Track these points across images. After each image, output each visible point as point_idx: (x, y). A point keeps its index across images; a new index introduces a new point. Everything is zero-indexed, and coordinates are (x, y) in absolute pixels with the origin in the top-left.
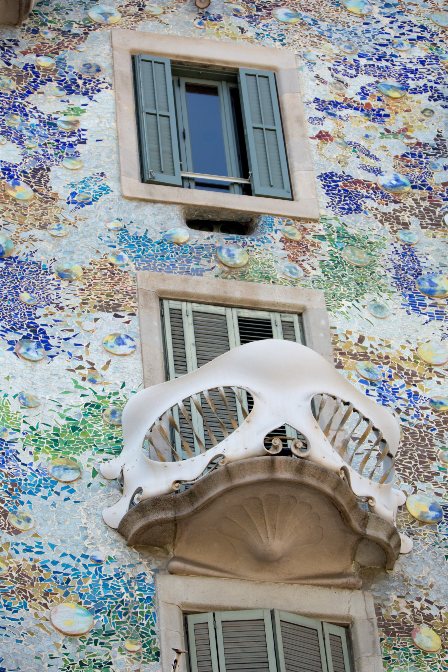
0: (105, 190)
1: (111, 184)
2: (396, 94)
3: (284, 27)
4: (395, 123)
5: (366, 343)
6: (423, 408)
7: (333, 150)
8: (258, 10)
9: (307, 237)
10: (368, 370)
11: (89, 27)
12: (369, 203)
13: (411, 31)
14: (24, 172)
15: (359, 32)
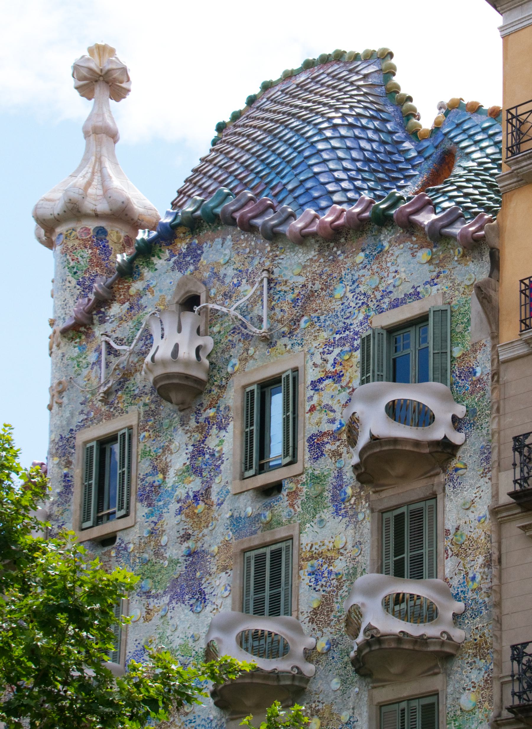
0: (228, 492)
1: (229, 488)
2: (347, 357)
3: (304, 332)
4: (345, 381)
5: (313, 549)
6: (333, 579)
7: (316, 416)
8: (295, 324)
9: (299, 486)
10: (312, 566)
11: (229, 376)
12: (328, 447)
13: (360, 300)
14: (202, 494)
15: (339, 314)
